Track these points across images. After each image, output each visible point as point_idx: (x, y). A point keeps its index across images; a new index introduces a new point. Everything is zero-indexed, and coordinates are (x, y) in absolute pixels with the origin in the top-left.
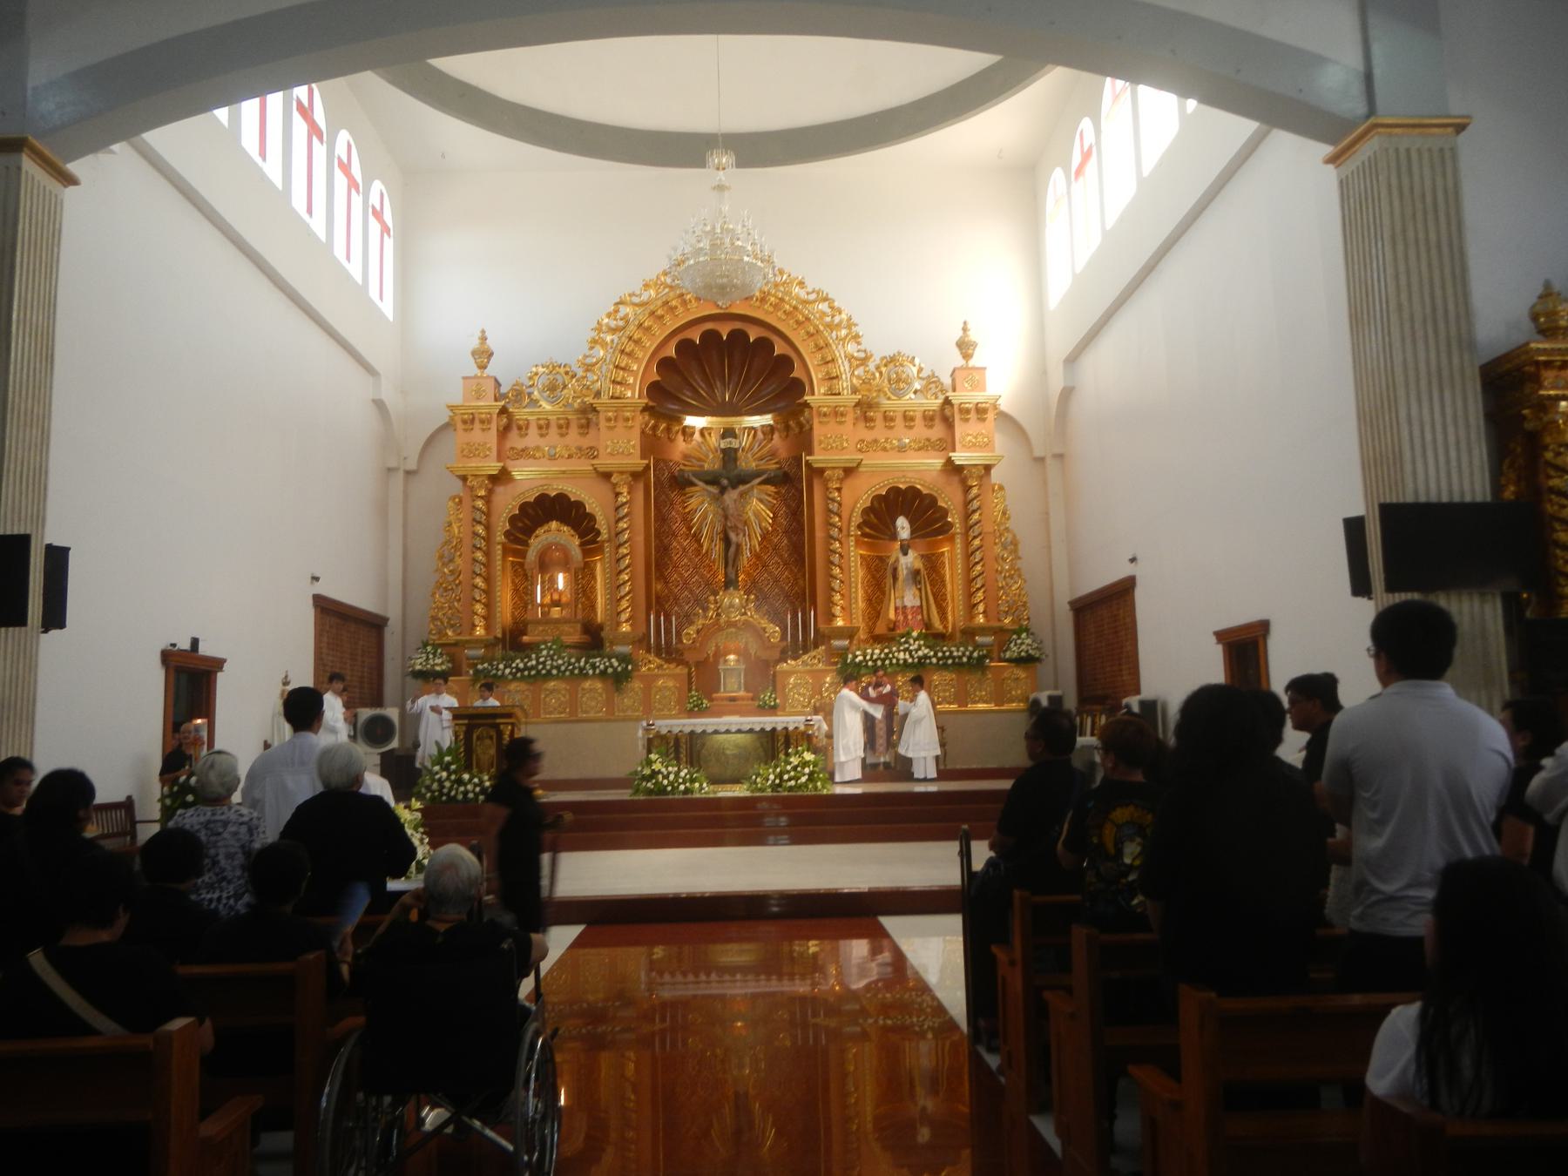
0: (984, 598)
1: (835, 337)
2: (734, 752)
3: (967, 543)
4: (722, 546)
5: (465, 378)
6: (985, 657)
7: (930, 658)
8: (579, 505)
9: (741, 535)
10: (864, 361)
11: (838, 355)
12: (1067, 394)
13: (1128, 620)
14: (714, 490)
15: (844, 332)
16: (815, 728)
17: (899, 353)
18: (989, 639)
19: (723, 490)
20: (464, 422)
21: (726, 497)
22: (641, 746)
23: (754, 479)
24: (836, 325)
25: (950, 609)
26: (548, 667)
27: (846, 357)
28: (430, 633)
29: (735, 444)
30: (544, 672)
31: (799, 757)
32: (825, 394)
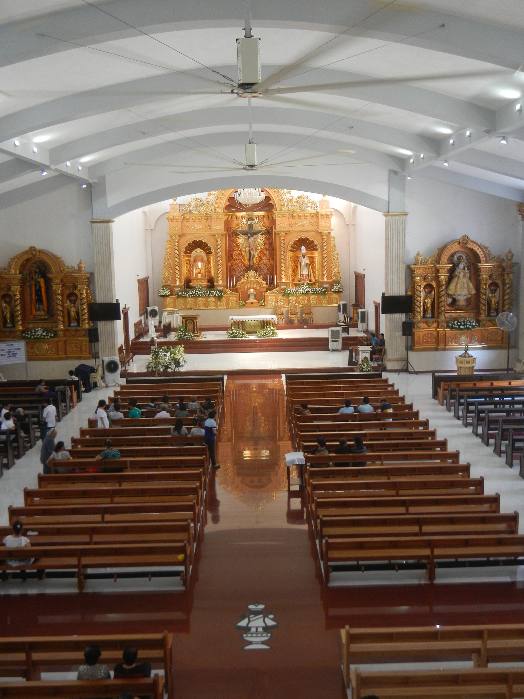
6: (326, 291)
18: (327, 286)
19: (249, 238)
21: (249, 240)
29: (252, 222)
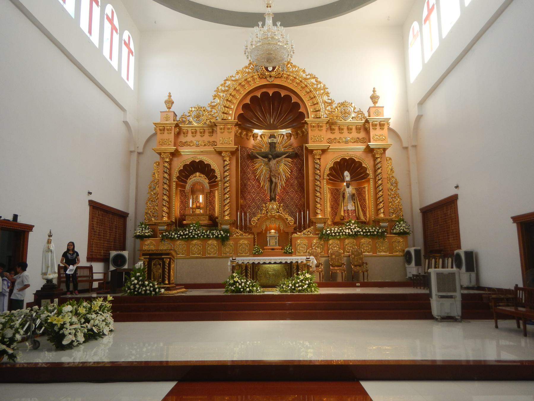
0: (383, 206)
1: (318, 94)
2: (273, 273)
3: (375, 183)
4: (269, 184)
5: (161, 112)
6: (384, 232)
7: (360, 232)
8: (209, 165)
9: (277, 179)
10: (330, 104)
11: (319, 101)
12: (419, 118)
13: (453, 215)
14: (266, 160)
15: (322, 91)
16: (311, 262)
17: (345, 101)
18: (386, 224)
19: (270, 160)
20: (160, 130)
21: (271, 163)
22: (229, 269)
23: (283, 155)
24: (319, 89)
25: (368, 211)
26: (193, 234)
27: (323, 102)
28: (145, 219)
29: (275, 140)
30: (191, 236)
31: (304, 276)
32: (314, 118)
